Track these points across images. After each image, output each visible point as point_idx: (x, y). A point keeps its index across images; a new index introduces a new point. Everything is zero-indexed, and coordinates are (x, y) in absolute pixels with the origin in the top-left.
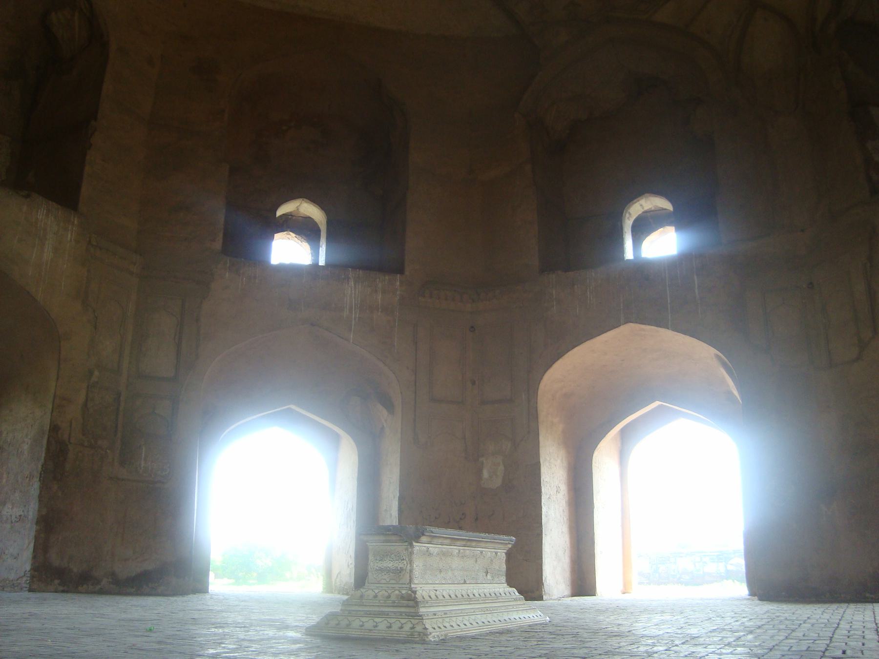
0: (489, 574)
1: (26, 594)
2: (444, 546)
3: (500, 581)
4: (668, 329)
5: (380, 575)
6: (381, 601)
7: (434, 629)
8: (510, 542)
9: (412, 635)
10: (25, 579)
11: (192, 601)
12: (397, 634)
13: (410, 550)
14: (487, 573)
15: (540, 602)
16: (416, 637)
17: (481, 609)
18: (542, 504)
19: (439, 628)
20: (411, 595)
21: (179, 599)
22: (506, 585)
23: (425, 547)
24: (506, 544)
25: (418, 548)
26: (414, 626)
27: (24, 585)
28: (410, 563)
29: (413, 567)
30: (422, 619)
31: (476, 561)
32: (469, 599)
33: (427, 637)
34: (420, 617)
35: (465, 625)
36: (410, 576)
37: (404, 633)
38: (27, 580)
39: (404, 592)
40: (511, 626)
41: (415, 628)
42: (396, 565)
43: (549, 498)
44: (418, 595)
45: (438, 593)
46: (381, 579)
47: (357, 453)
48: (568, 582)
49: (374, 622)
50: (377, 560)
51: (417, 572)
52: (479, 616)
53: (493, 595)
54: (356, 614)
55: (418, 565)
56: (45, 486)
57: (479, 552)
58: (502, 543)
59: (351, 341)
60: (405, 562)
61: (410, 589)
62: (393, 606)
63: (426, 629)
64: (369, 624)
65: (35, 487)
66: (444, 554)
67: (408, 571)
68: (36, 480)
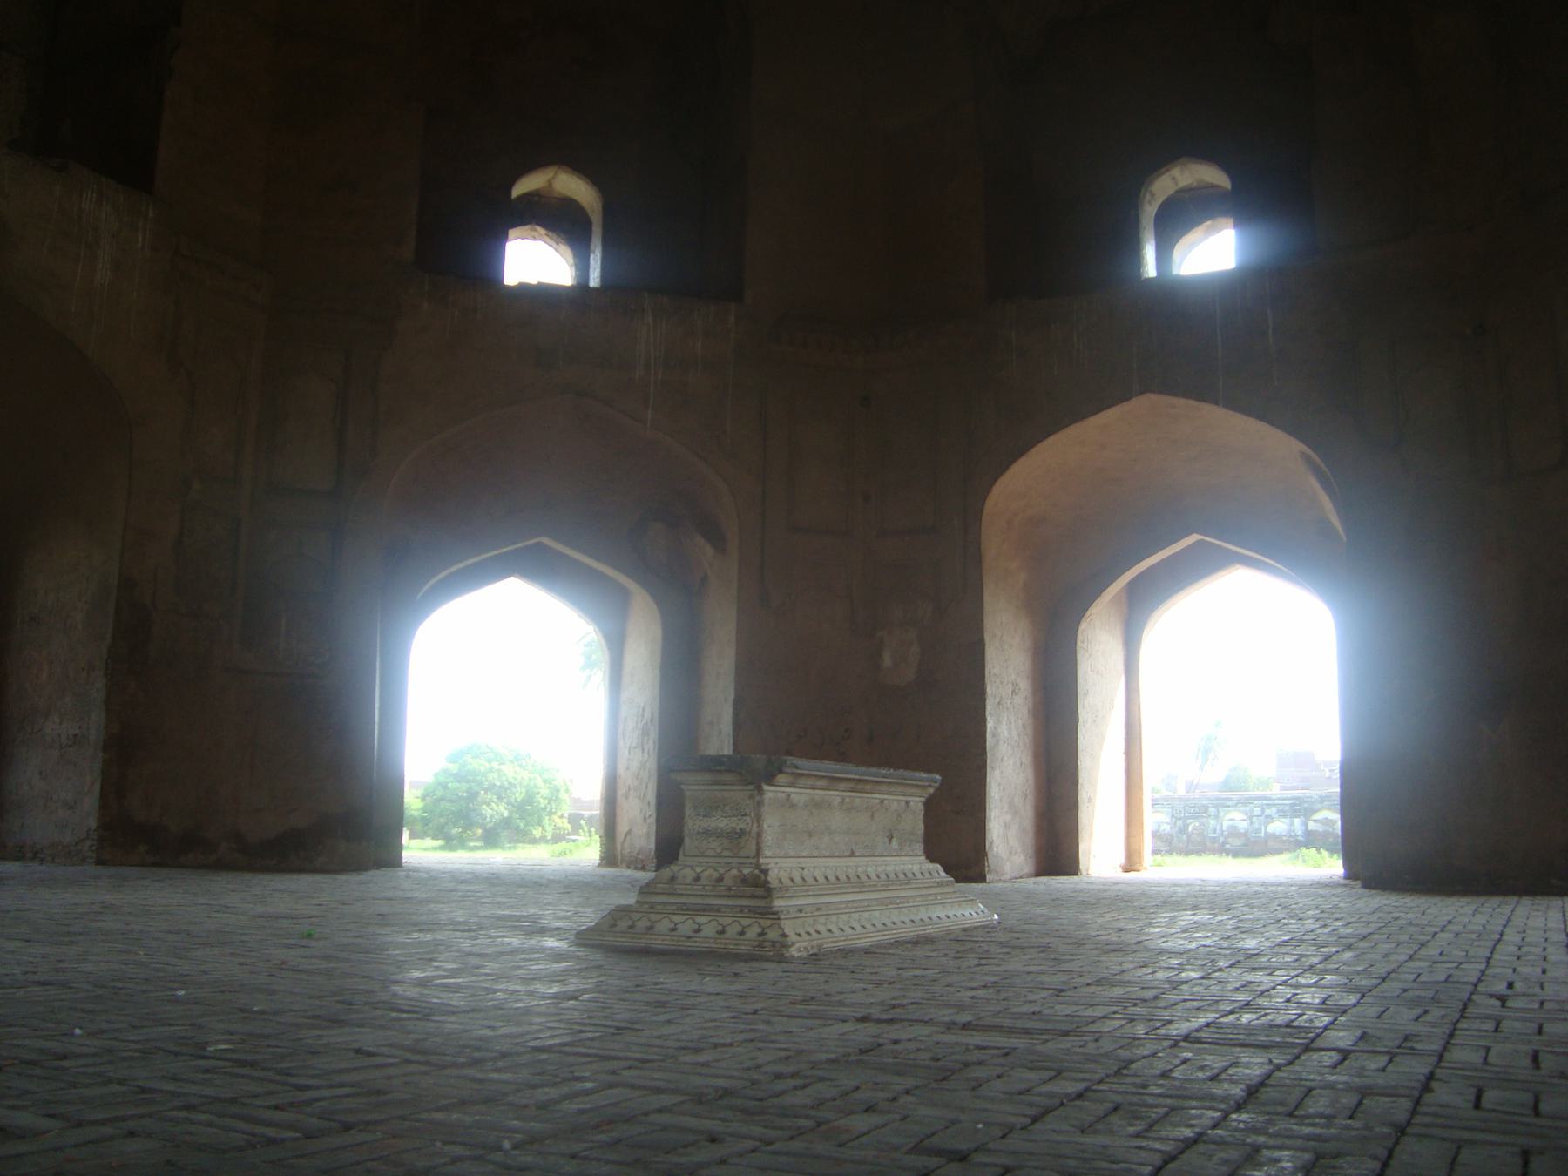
0: (894, 839)
1: (92, 869)
2: (817, 791)
3: (913, 851)
5: (705, 842)
6: (707, 888)
7: (799, 935)
8: (933, 784)
9: (761, 946)
10: (88, 843)
11: (373, 882)
13: (757, 798)
14: (891, 838)
15: (981, 885)
18: (987, 713)
19: (808, 933)
20: (759, 877)
22: (923, 858)
23: (784, 792)
24: (925, 787)
25: (771, 795)
28: (758, 822)
29: (762, 827)
30: (779, 919)
31: (872, 816)
32: (859, 883)
34: (775, 915)
35: (853, 928)
36: (758, 844)
37: (746, 942)
38: (93, 845)
39: (746, 871)
40: (932, 931)
42: (733, 825)
43: (999, 703)
44: (772, 877)
45: (806, 872)
46: (707, 849)
48: (1031, 852)
49: (695, 923)
50: (699, 815)
51: (769, 837)
52: (877, 913)
53: (902, 876)
55: (771, 824)
58: (918, 786)
61: (758, 866)
62: (729, 896)
63: (784, 936)
64: (686, 927)
66: (818, 805)
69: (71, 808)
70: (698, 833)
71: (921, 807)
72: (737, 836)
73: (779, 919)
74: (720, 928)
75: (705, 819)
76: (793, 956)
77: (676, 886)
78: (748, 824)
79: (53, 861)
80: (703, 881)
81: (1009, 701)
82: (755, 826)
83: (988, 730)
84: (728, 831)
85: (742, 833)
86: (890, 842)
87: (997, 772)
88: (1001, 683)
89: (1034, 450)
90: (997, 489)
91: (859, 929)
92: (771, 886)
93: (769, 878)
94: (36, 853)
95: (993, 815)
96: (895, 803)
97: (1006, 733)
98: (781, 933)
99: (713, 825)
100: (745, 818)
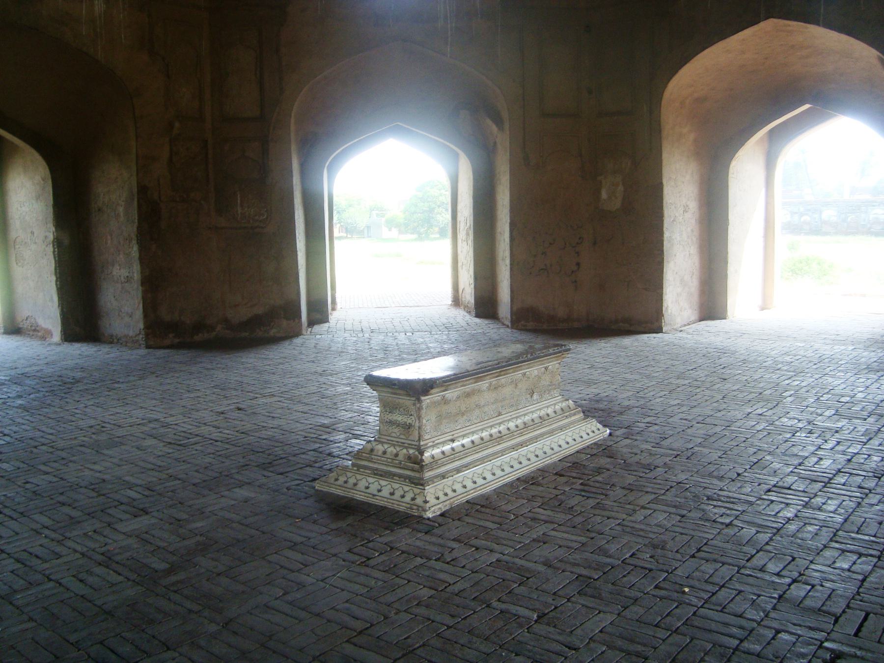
5: (390, 428)
10: (141, 336)
12: (398, 505)
13: (418, 405)
14: (533, 393)
15: (660, 335)
18: (664, 229)
26: (416, 497)
36: (419, 433)
37: (404, 504)
39: (411, 451)
42: (405, 420)
43: (674, 221)
56: (142, 249)
59: (449, 55)
60: (413, 419)
63: (426, 502)
65: (135, 250)
66: (468, 395)
67: (417, 428)
68: (134, 242)
70: (387, 422)
73: (424, 489)
74: (392, 491)
77: (373, 457)
80: (388, 455)
81: (681, 218)
82: (417, 421)
86: (532, 396)
88: (675, 207)
89: (695, 58)
92: (424, 464)
93: (424, 458)
95: (668, 291)
98: (424, 500)
99: (395, 418)
100: (411, 417)
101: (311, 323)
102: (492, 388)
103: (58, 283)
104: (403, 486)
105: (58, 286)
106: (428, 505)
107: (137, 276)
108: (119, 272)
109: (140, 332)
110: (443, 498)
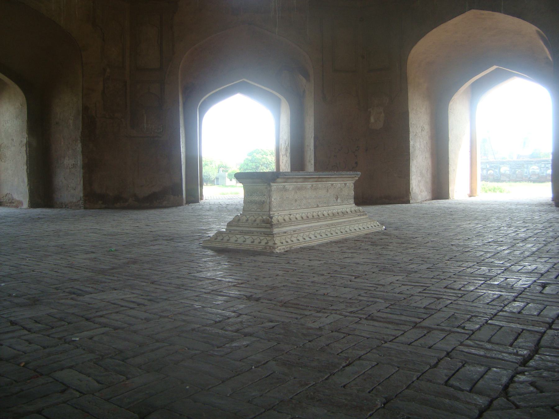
0: (339, 199)
1: (82, 211)
3: (349, 202)
4: (501, 12)
6: (250, 224)
8: (356, 176)
11: (186, 210)
14: (337, 198)
16: (267, 249)
17: (327, 225)
18: (410, 139)
19: (287, 242)
20: (269, 219)
21: (174, 209)
22: (354, 205)
23: (281, 185)
24: (353, 177)
25: (275, 187)
27: (82, 205)
28: (269, 197)
29: (272, 200)
30: (274, 237)
31: (328, 191)
33: (275, 250)
34: (271, 234)
36: (269, 207)
37: (261, 246)
38: (82, 203)
39: (264, 217)
40: (350, 236)
41: (268, 243)
42: (261, 199)
43: (415, 135)
44: (274, 220)
45: (292, 216)
47: (289, 108)
52: (324, 231)
54: (234, 233)
55: (275, 198)
56: (84, 146)
57: (330, 185)
58: (350, 177)
59: (277, 33)
60: (266, 197)
62: (258, 227)
63: (275, 244)
64: (240, 240)
65: (79, 147)
66: (299, 189)
67: (268, 203)
68: (79, 141)
69: (75, 190)
70: (248, 202)
71: (352, 185)
72: (262, 203)
74: (253, 240)
75: (251, 197)
76: (277, 253)
77: (239, 223)
78: (265, 199)
79: (71, 208)
80: (249, 221)
81: (420, 134)
82: (268, 199)
83: (411, 145)
84: (259, 201)
85: (264, 202)
86: (337, 200)
87: (415, 162)
88: (416, 127)
90: (413, 51)
91: (313, 237)
92: (273, 223)
93: (273, 220)
94: (66, 205)
95: (413, 178)
96: (339, 184)
97: (418, 146)
99: (254, 199)
100: (264, 196)
101: (188, 202)
102: (313, 188)
103: (28, 170)
104: (259, 237)
105: (28, 172)
106: (276, 245)
107: (80, 163)
108: (68, 162)
109: (81, 199)
110: (285, 243)
